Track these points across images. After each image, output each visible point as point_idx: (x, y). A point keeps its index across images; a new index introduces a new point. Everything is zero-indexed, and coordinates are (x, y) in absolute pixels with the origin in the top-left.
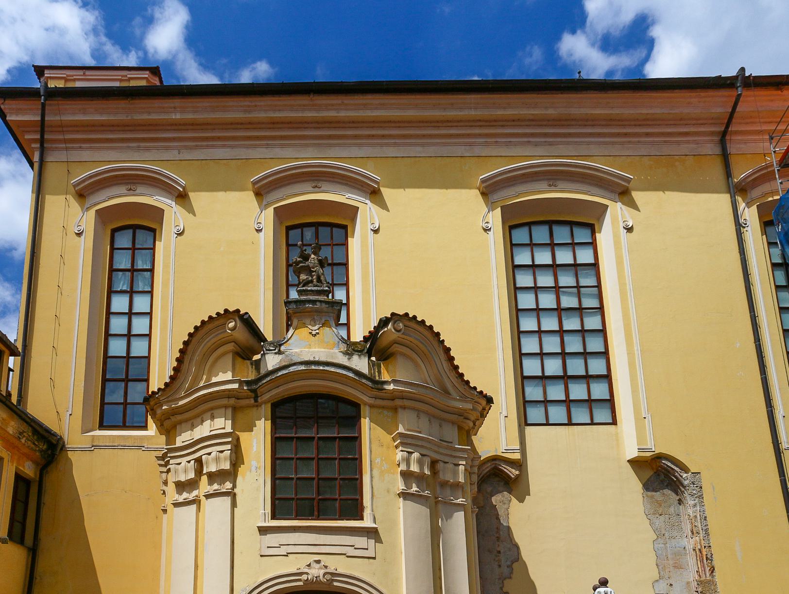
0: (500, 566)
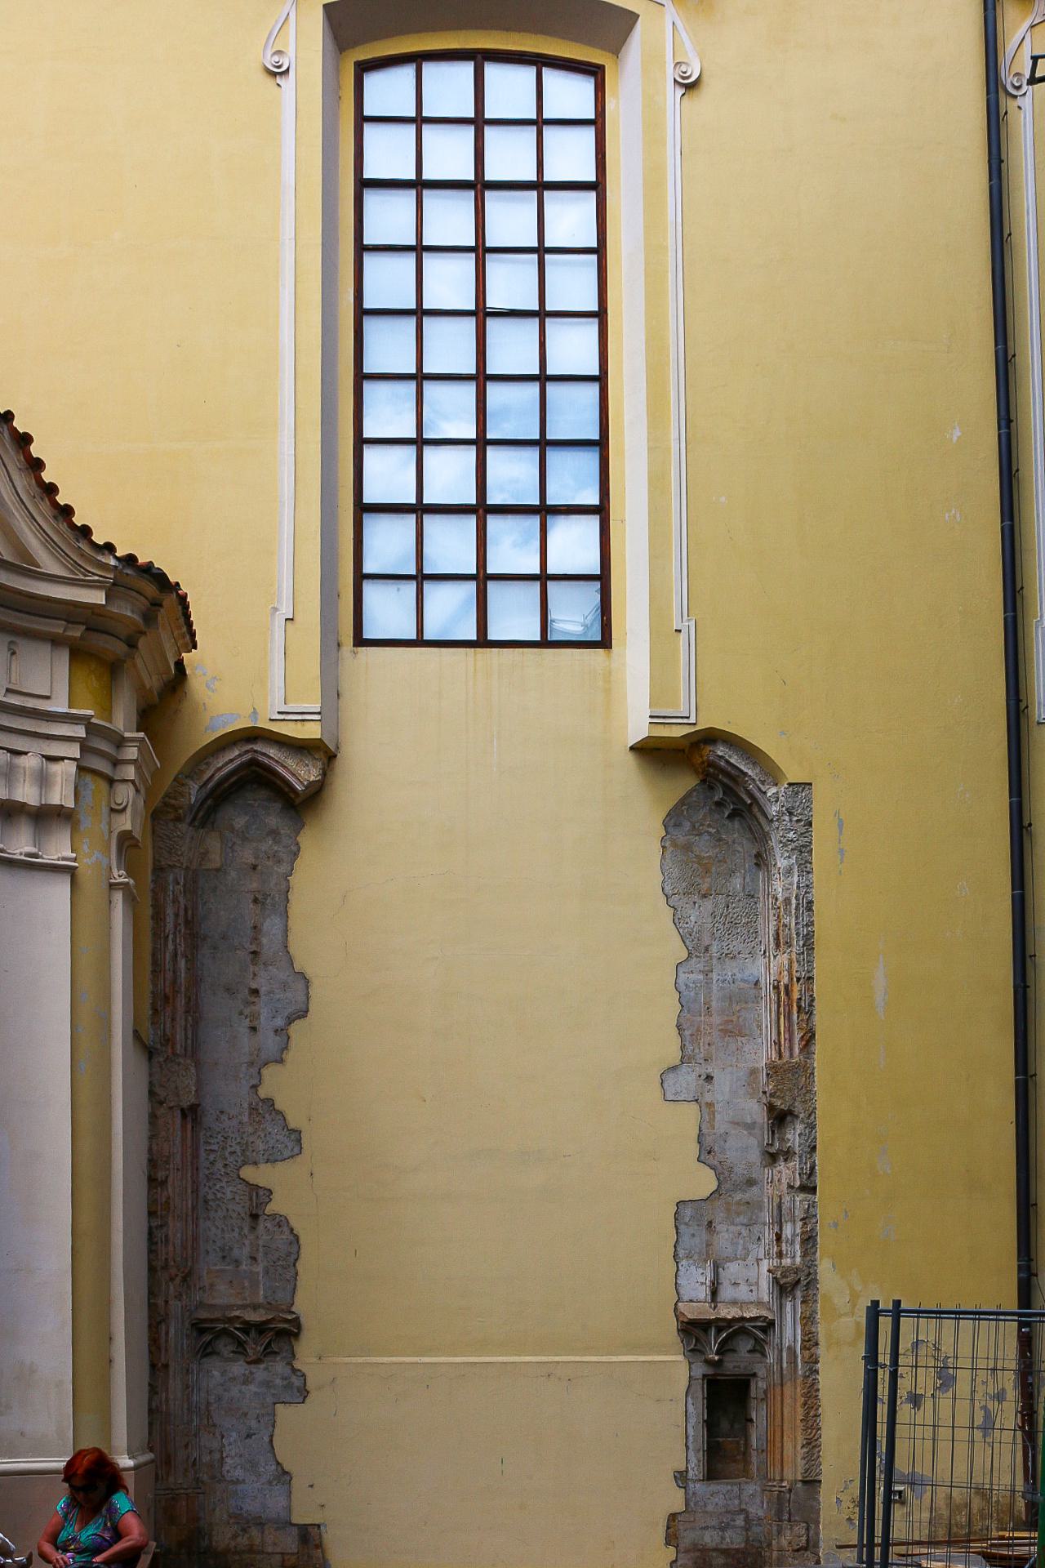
0: (254, 1029)
